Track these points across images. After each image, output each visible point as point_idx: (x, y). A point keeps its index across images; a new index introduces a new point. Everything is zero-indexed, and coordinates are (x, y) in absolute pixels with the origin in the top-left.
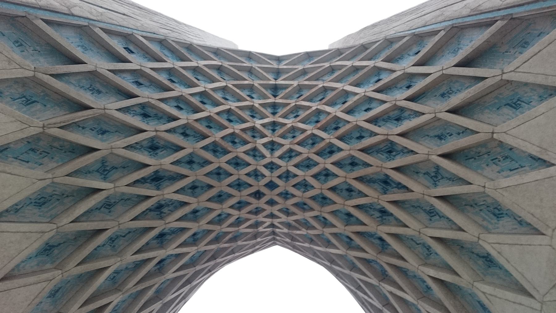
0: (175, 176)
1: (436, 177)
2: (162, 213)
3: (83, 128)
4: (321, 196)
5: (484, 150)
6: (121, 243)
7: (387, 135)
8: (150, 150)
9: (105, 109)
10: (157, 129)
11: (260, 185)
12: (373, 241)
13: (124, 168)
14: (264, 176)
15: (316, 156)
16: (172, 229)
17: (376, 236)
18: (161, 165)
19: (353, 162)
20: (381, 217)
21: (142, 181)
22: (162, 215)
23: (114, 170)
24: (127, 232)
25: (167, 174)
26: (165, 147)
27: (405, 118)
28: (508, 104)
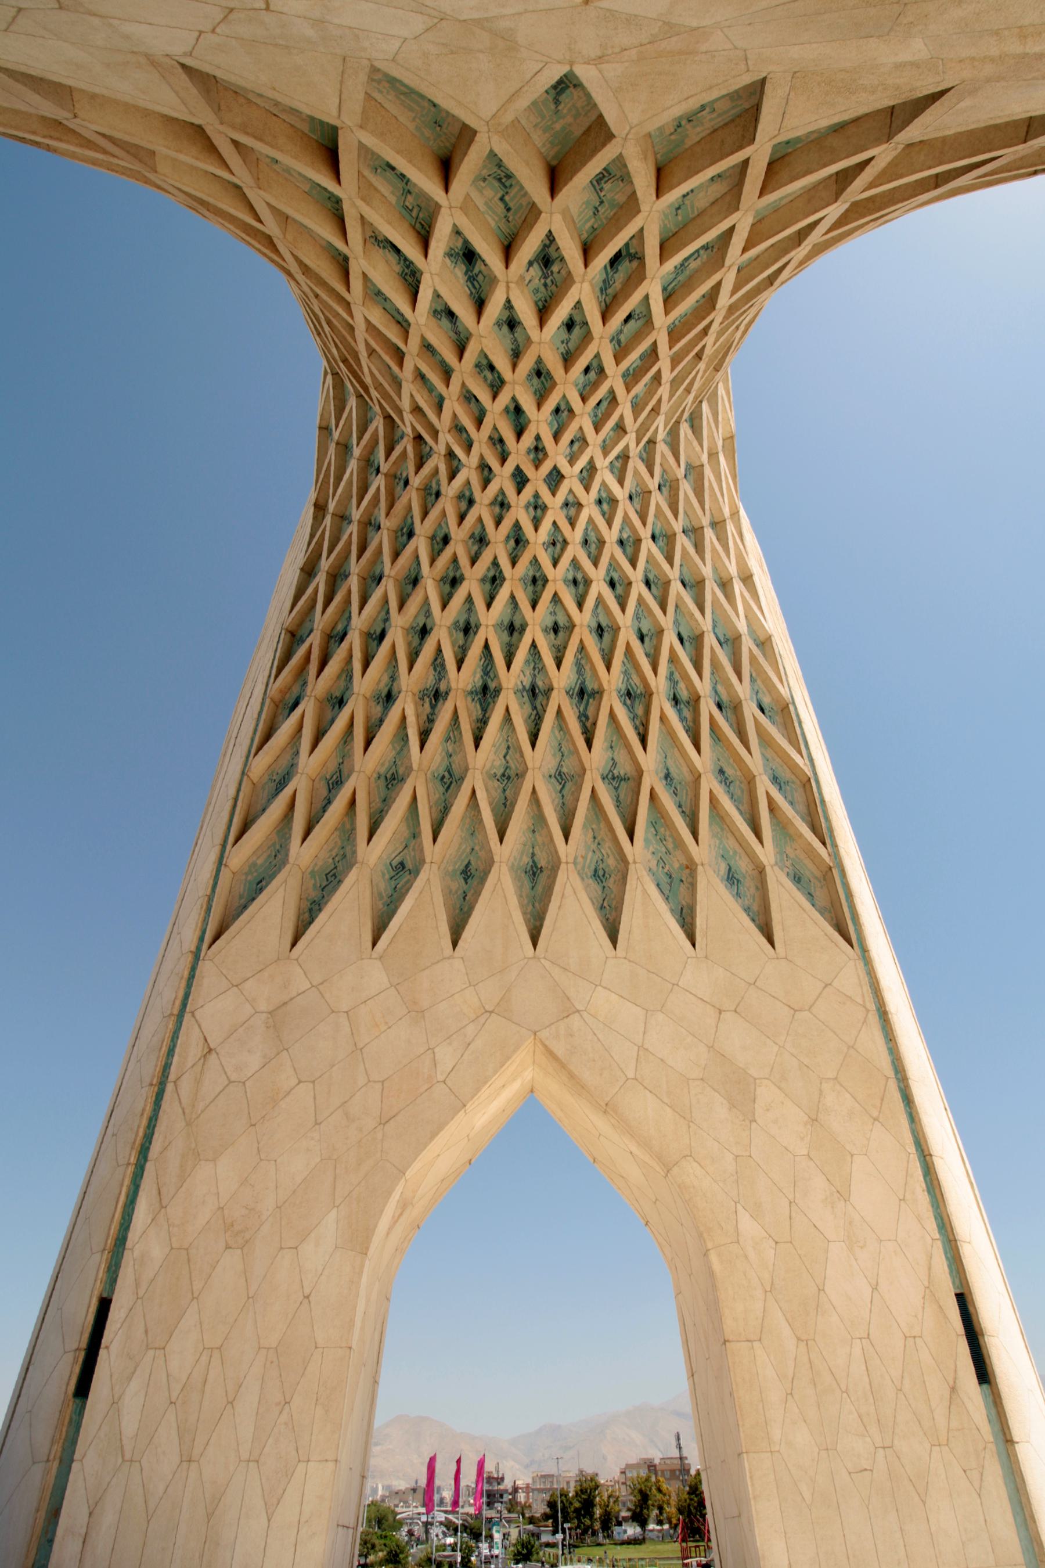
0: (609, 291)
1: (614, 778)
4: (538, 575)
5: (670, 846)
6: (489, 193)
7: (658, 693)
11: (557, 455)
12: (478, 676)
13: (678, 208)
14: (572, 461)
15: (607, 560)
16: (480, 278)
17: (489, 681)
19: (602, 630)
20: (524, 687)
24: (511, 205)
27: (680, 711)
28: (730, 870)
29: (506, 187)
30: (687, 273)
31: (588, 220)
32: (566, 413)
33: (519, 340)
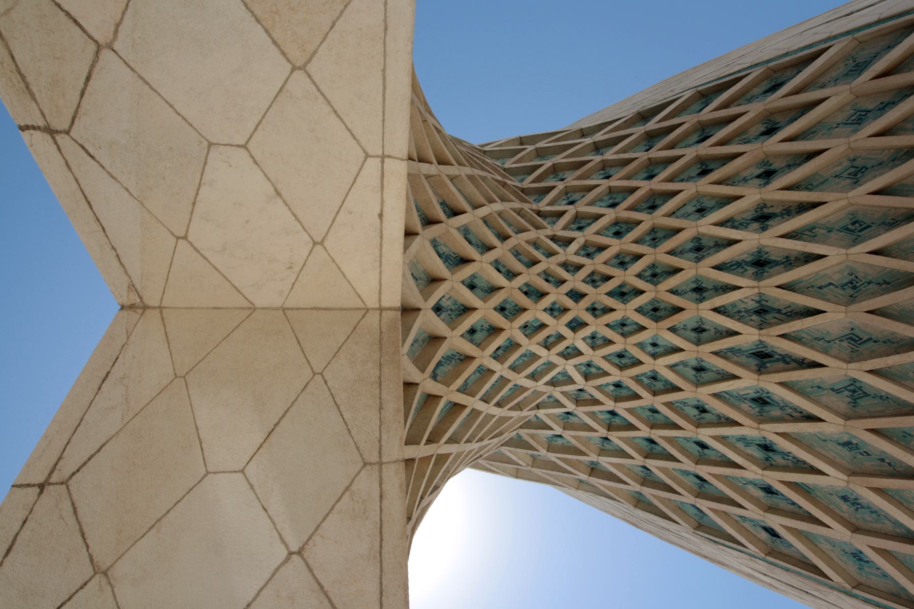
0: (729, 354)
2: (758, 302)
3: (883, 460)
4: (506, 312)
8: (768, 400)
9: (848, 482)
10: (757, 432)
13: (819, 387)
14: (584, 339)
16: (740, 270)
18: (758, 380)
21: (788, 360)
22: (757, 299)
23: (836, 388)
24: (825, 289)
25: (743, 359)
26: (742, 398)
29: (843, 286)
30: (737, 403)
31: (809, 335)
32: (621, 331)
33: (686, 295)
